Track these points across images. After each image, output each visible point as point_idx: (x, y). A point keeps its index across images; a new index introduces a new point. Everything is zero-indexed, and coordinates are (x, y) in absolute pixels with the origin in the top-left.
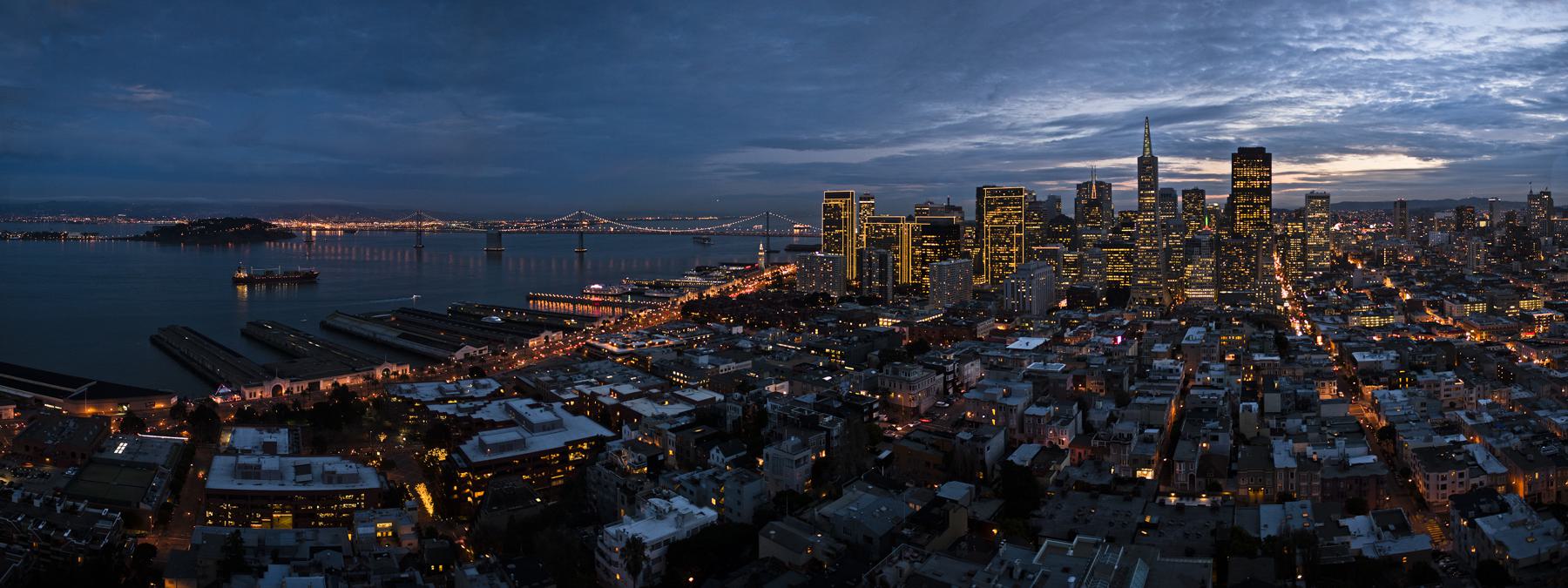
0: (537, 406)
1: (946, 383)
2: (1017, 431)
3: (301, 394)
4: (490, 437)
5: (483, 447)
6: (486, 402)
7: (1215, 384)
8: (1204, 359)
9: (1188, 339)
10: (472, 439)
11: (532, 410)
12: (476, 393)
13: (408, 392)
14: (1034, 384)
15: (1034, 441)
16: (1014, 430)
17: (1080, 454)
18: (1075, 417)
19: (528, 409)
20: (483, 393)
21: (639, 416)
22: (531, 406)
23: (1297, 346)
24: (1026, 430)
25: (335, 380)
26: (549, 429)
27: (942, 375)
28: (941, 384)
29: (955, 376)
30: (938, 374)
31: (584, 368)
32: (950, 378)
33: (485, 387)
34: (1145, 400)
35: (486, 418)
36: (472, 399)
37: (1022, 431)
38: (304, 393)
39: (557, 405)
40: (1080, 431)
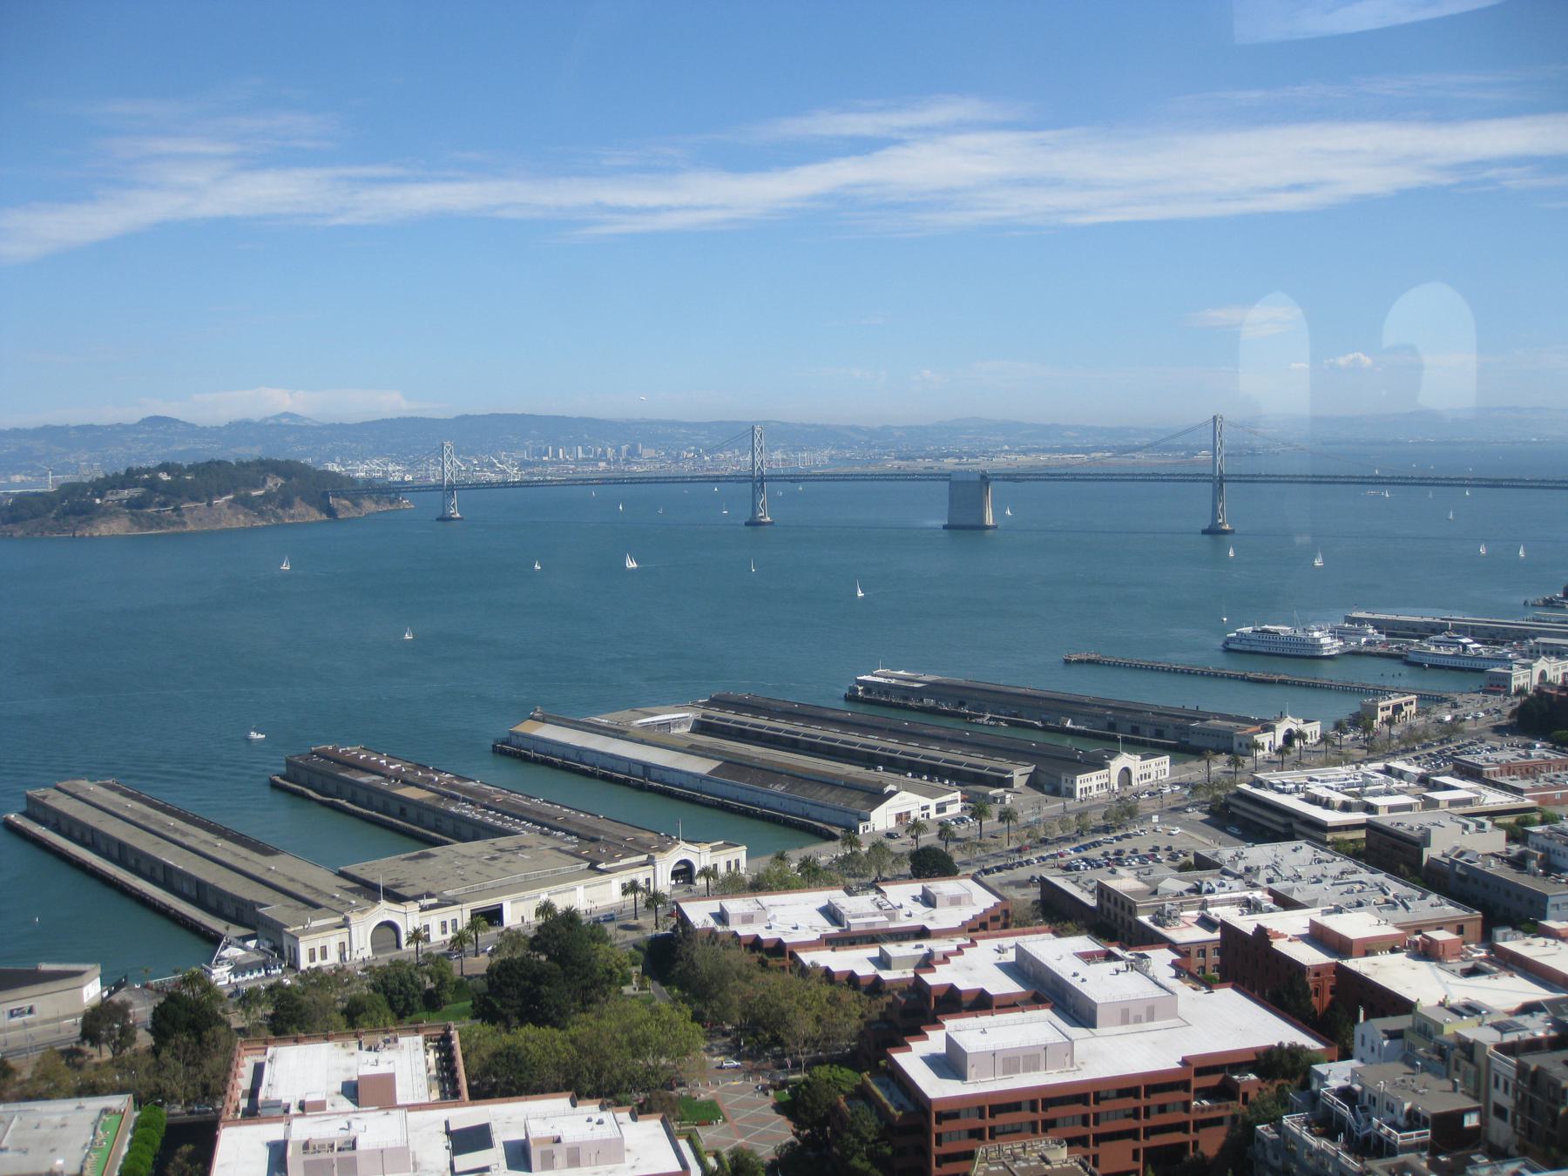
0: (1110, 956)
3: (453, 940)
4: (969, 1032)
5: (950, 1064)
6: (960, 941)
10: (926, 1038)
11: (1093, 966)
12: (932, 918)
13: (748, 919)
19: (1079, 965)
20: (945, 917)
21: (1403, 1006)
22: (1088, 957)
25: (544, 897)
26: (1138, 1020)
31: (1233, 861)
33: (955, 901)
35: (963, 985)
36: (922, 933)
38: (459, 940)
39: (1160, 959)
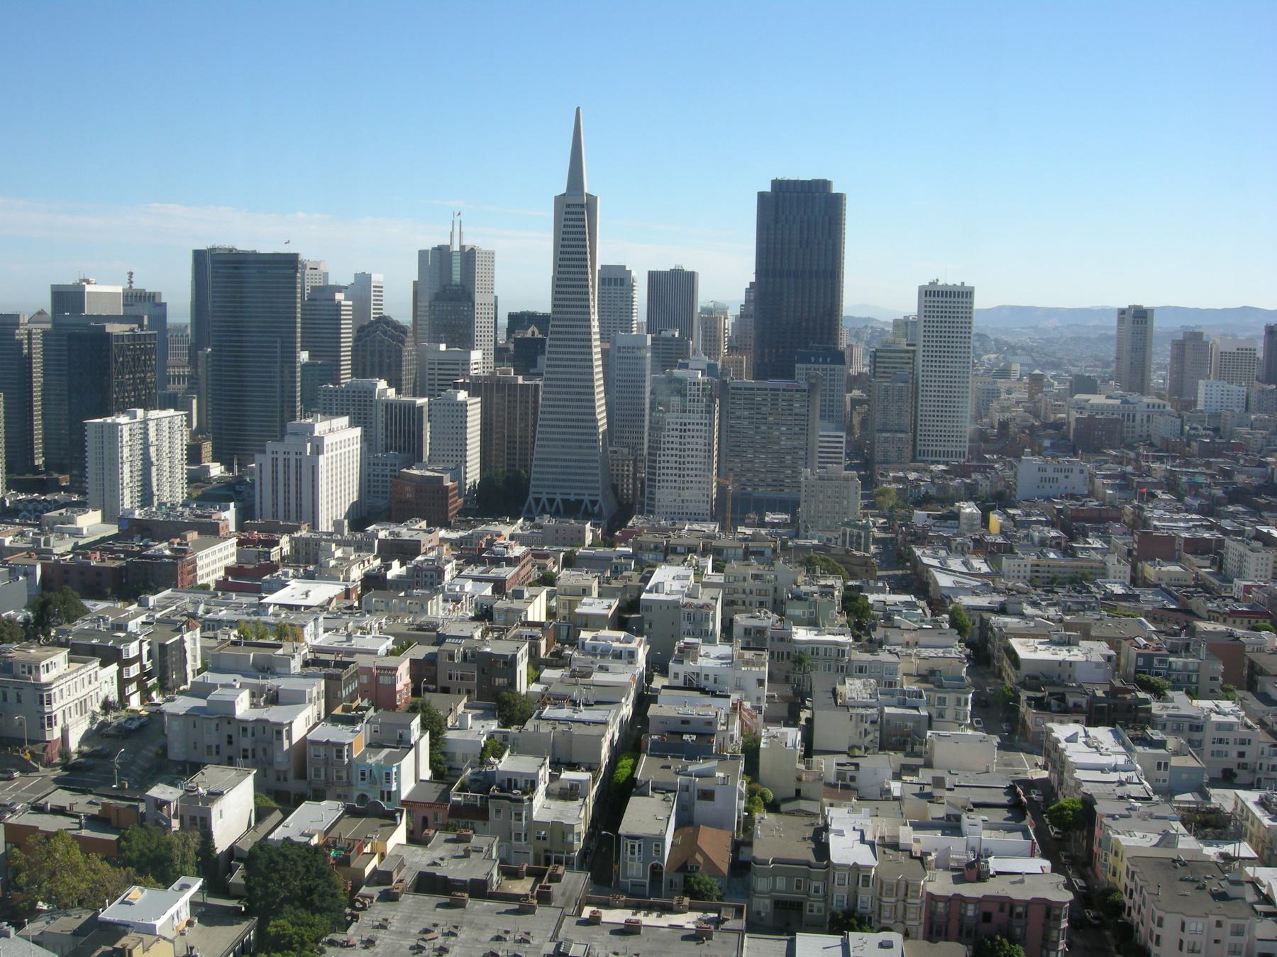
1: (123, 683)
2: (291, 775)
7: (709, 684)
8: (689, 634)
9: (656, 589)
14: (328, 678)
15: (328, 793)
16: (285, 772)
17: (425, 820)
18: (417, 743)
23: (888, 618)
24: (311, 771)
27: (114, 668)
28: (112, 692)
29: (143, 667)
30: (104, 664)
32: (134, 670)
34: (565, 712)
37: (302, 774)
40: (426, 774)
